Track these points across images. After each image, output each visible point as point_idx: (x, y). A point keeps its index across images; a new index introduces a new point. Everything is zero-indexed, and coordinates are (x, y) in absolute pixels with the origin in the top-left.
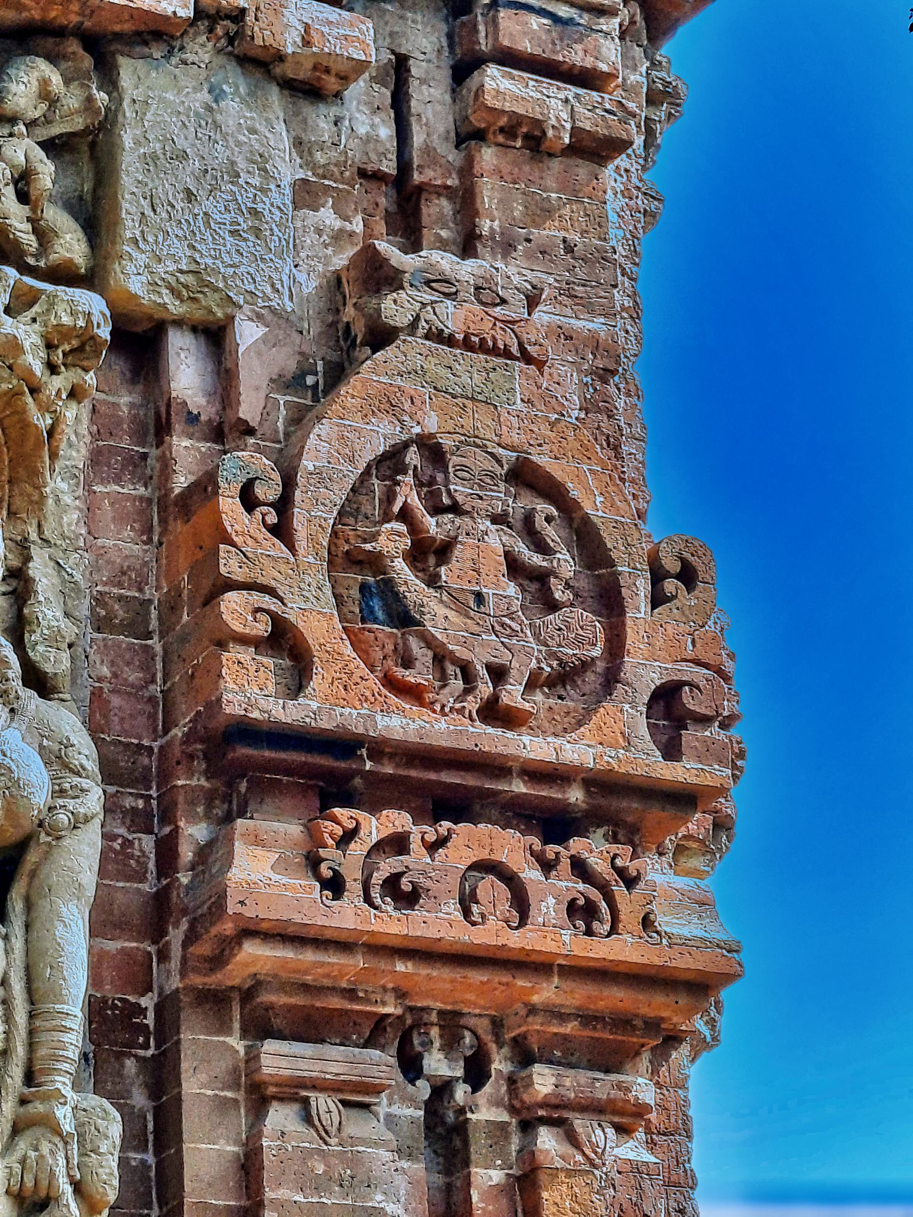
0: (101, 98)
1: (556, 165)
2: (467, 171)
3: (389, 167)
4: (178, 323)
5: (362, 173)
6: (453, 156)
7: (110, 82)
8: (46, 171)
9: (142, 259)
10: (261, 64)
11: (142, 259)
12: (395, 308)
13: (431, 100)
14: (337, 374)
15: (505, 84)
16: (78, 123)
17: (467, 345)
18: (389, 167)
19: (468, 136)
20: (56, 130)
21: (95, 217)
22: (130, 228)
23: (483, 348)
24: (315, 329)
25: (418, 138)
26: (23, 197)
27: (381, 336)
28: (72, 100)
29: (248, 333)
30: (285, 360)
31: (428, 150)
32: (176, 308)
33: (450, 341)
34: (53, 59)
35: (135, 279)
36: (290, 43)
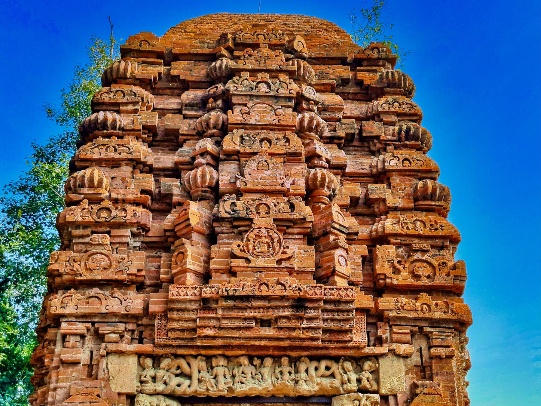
0: (377, 365)
1: (444, 360)
2: (431, 363)
3: (420, 364)
4: (390, 395)
5: (415, 366)
6: (429, 361)
7: (378, 363)
8: (371, 376)
9: (384, 388)
10: (399, 356)
11: (384, 388)
12: (418, 391)
13: (425, 353)
14: (412, 399)
15: (435, 351)
16: (375, 369)
17: (429, 394)
18: (420, 364)
19: (431, 358)
20: (372, 370)
21: (377, 381)
22: (382, 383)
23: (431, 394)
24: (409, 393)
25: (424, 359)
26: (368, 381)
27: (417, 395)
28: (374, 366)
29: (399, 396)
30: (405, 399)
31: (425, 361)
32: (389, 393)
33: (426, 394)
34: (370, 360)
35: (383, 391)
36: (402, 352)
